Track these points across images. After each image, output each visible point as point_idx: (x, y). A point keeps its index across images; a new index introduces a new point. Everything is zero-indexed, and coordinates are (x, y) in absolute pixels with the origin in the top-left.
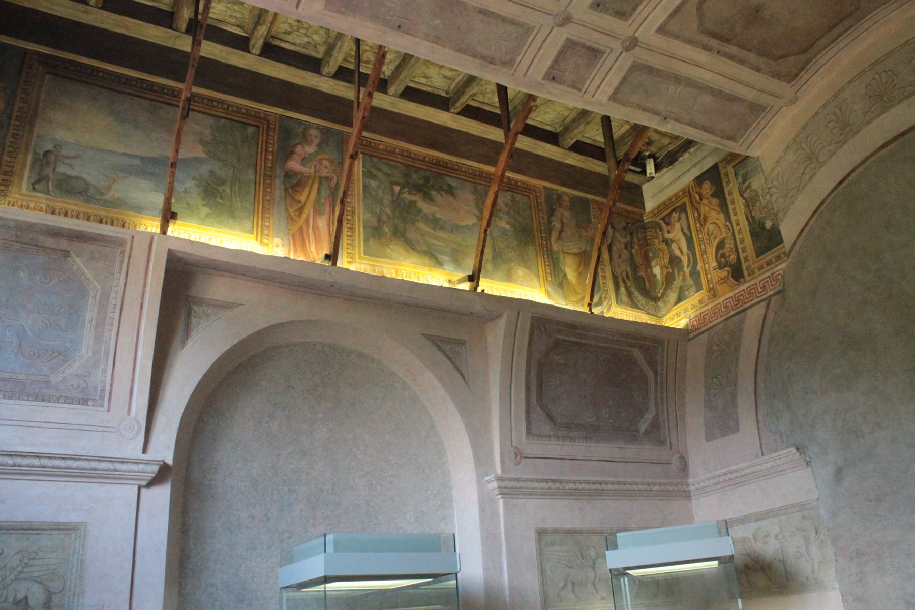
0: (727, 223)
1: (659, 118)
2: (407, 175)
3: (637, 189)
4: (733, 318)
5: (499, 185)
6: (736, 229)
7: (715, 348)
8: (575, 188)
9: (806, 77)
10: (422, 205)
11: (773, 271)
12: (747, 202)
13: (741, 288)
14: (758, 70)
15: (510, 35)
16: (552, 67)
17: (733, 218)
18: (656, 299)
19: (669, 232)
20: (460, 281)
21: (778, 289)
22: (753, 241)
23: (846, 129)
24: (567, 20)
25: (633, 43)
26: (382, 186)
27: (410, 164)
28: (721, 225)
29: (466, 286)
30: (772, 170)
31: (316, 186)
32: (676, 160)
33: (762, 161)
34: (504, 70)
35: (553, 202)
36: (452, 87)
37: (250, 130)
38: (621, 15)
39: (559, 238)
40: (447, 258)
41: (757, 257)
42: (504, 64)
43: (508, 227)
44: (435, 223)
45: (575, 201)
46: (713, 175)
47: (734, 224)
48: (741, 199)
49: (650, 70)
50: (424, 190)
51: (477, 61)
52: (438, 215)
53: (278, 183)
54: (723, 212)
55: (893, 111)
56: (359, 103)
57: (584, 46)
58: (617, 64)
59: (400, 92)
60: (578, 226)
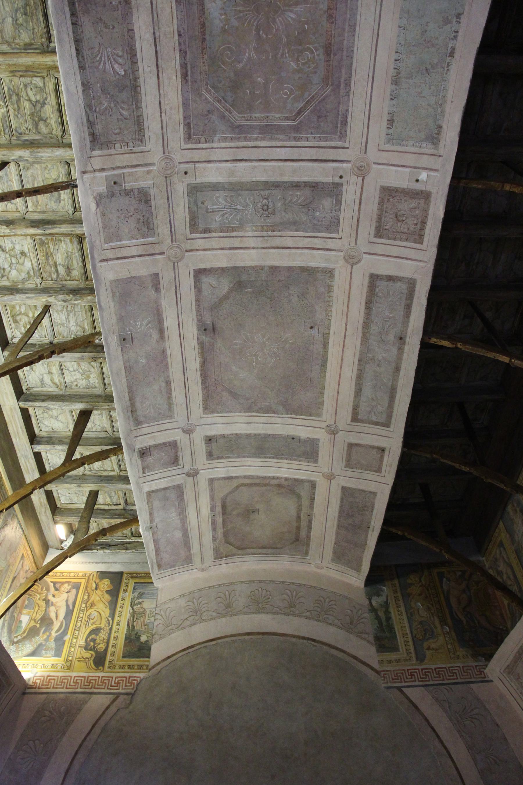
0: (110, 619)
1: (149, 525)
4: (77, 695)
6: (115, 627)
7: (47, 713)
9: (223, 562)
11: (132, 675)
12: (134, 612)
15: (159, 409)
16: (150, 447)
17: (117, 618)
19: (54, 596)
21: (129, 691)
22: (125, 645)
24: (188, 431)
32: (91, 549)
33: (159, 593)
34: (132, 423)
36: (35, 389)
38: (210, 455)
41: (123, 657)
46: (116, 579)
48: (130, 608)
51: (128, 403)
54: (110, 609)
55: (262, 617)
57: (177, 452)
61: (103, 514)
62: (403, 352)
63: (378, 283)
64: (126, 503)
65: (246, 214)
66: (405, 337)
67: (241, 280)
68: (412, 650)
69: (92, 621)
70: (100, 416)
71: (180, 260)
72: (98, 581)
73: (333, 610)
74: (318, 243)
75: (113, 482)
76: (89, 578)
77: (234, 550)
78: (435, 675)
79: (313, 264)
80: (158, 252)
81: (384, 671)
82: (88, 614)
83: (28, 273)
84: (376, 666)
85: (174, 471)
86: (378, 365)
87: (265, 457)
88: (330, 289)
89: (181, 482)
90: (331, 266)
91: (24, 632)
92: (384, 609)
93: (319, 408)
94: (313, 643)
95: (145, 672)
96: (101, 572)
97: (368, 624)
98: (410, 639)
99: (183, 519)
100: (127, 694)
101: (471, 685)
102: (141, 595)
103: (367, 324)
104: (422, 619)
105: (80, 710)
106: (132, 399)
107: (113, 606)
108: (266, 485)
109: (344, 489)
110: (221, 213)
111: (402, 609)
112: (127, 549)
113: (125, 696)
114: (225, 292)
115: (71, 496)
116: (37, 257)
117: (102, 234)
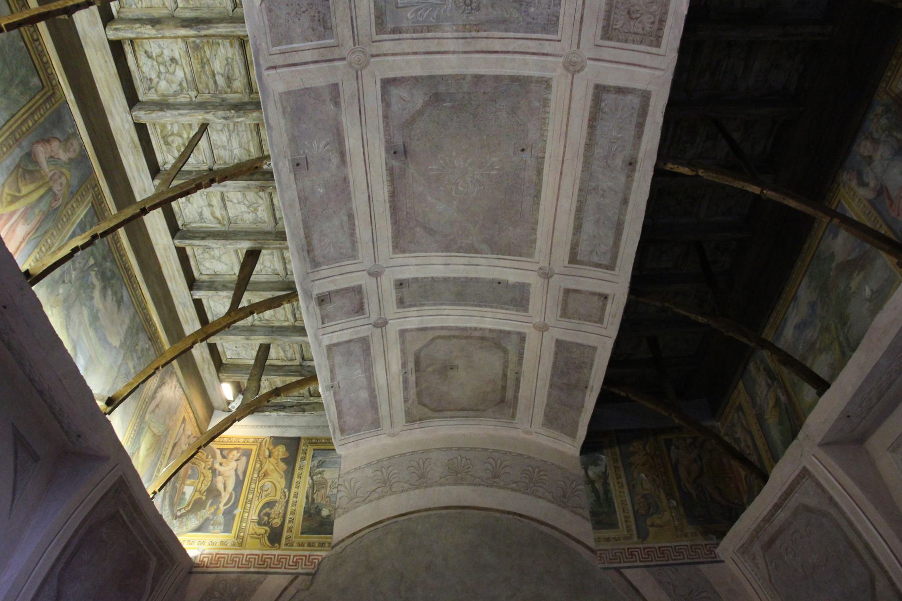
1: (330, 383)
2: (104, 258)
4: (250, 575)
6: (292, 500)
7: (217, 594)
9: (416, 426)
10: (97, 294)
11: (312, 553)
13: (273, 552)
16: (330, 293)
17: (294, 490)
19: (221, 464)
21: (309, 571)
22: (304, 520)
24: (375, 274)
30: (348, 472)
31: (42, 191)
32: (263, 411)
34: (309, 265)
36: (194, 225)
37: (35, 81)
38: (401, 303)
41: (302, 533)
44: (95, 318)
46: (293, 445)
48: (309, 478)
51: (304, 241)
52: (100, 315)
53: (17, 153)
57: (362, 299)
61: (276, 371)
62: (632, 180)
63: (605, 96)
64: (303, 359)
65: (445, 11)
66: (636, 162)
67: (438, 92)
68: (634, 527)
69: (265, 493)
70: (270, 257)
71: (365, 67)
72: (271, 447)
74: (532, 46)
75: (286, 333)
76: (261, 444)
77: (430, 413)
79: (526, 72)
80: (337, 57)
82: (260, 485)
83: (180, 84)
84: (591, 543)
85: (360, 320)
86: (602, 196)
87: (466, 305)
88: (545, 103)
89: (366, 334)
90: (547, 75)
91: (188, 505)
93: (531, 247)
96: (276, 438)
97: (584, 498)
98: (631, 515)
100: (307, 574)
101: (701, 567)
102: (321, 464)
103: (589, 146)
104: (646, 492)
105: (255, 591)
106: (308, 236)
108: (466, 338)
109: (559, 343)
110: (414, 8)
111: (623, 480)
112: (304, 411)
113: (305, 577)
114: (419, 106)
115: (238, 349)
116: (191, 65)
117: (268, 36)
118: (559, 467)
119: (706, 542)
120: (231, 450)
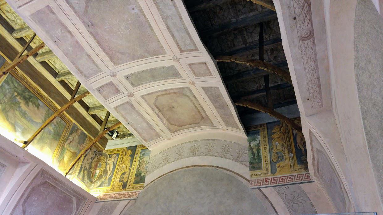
0: (130, 167)
2: (24, 91)
3: (107, 140)
5: (59, 115)
6: (132, 170)
7: (104, 209)
8: (85, 129)
10: (23, 106)
14: (164, 124)
16: (101, 87)
17: (133, 166)
18: (92, 182)
19: (109, 160)
20: (19, 141)
21: (135, 198)
23: (180, 156)
24: (114, 76)
25: (131, 95)
26: (10, 89)
27: (27, 88)
28: (127, 166)
29: (22, 145)
32: (125, 138)
34: (84, 78)
35: (74, 130)
36: (62, 71)
38: (133, 85)
39: (69, 144)
40: (20, 130)
41: (134, 183)
42: (85, 76)
43: (52, 130)
44: (24, 114)
45: (82, 133)
46: (134, 149)
47: (132, 168)
49: (132, 106)
50: (27, 100)
51: (76, 69)
52: (26, 112)
55: (195, 158)
56: (21, 55)
57: (115, 87)
58: (123, 98)
59: (41, 61)
60: (79, 143)
69: (123, 169)
73: (230, 151)
76: (123, 150)
77: (179, 128)
78: (280, 181)
81: (252, 180)
84: (248, 177)
87: (159, 80)
92: (257, 148)
94: (217, 168)
95: (142, 189)
97: (247, 157)
99: (142, 117)
100: (134, 199)
107: (132, 161)
108: (169, 94)
111: (267, 147)
113: (133, 200)
114: (85, 4)
118: (237, 144)
119: (306, 173)
120: (113, 154)
